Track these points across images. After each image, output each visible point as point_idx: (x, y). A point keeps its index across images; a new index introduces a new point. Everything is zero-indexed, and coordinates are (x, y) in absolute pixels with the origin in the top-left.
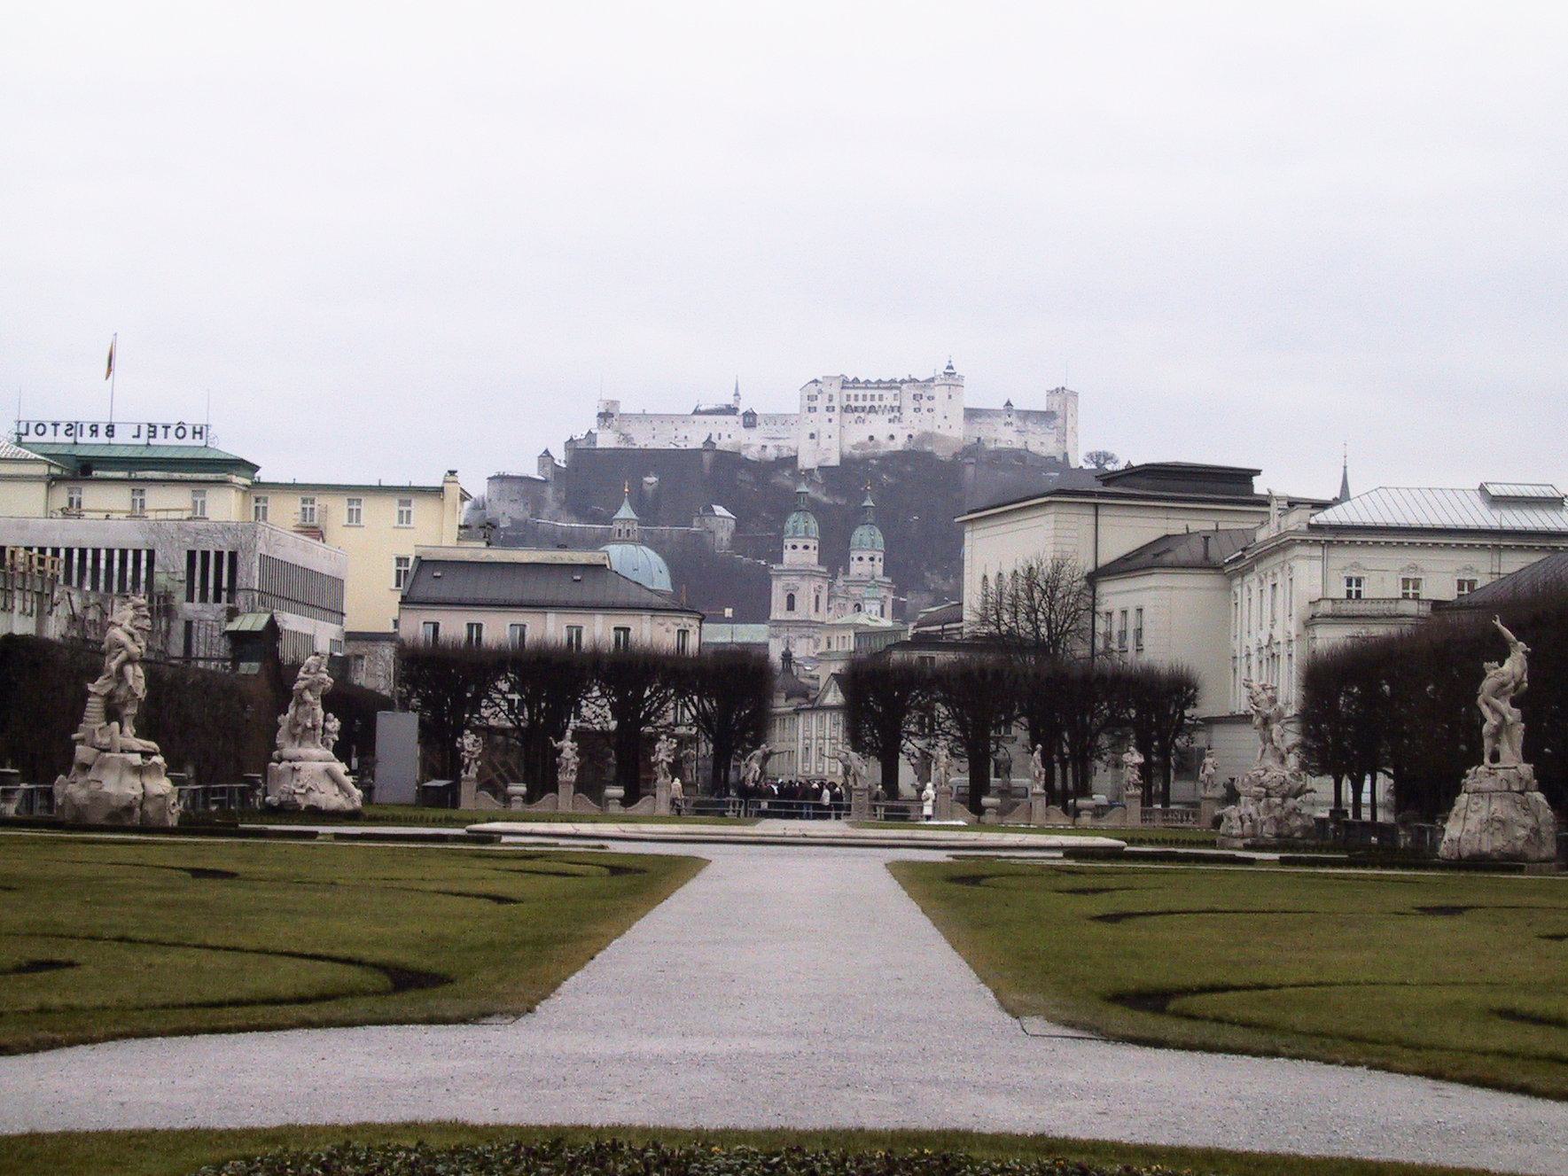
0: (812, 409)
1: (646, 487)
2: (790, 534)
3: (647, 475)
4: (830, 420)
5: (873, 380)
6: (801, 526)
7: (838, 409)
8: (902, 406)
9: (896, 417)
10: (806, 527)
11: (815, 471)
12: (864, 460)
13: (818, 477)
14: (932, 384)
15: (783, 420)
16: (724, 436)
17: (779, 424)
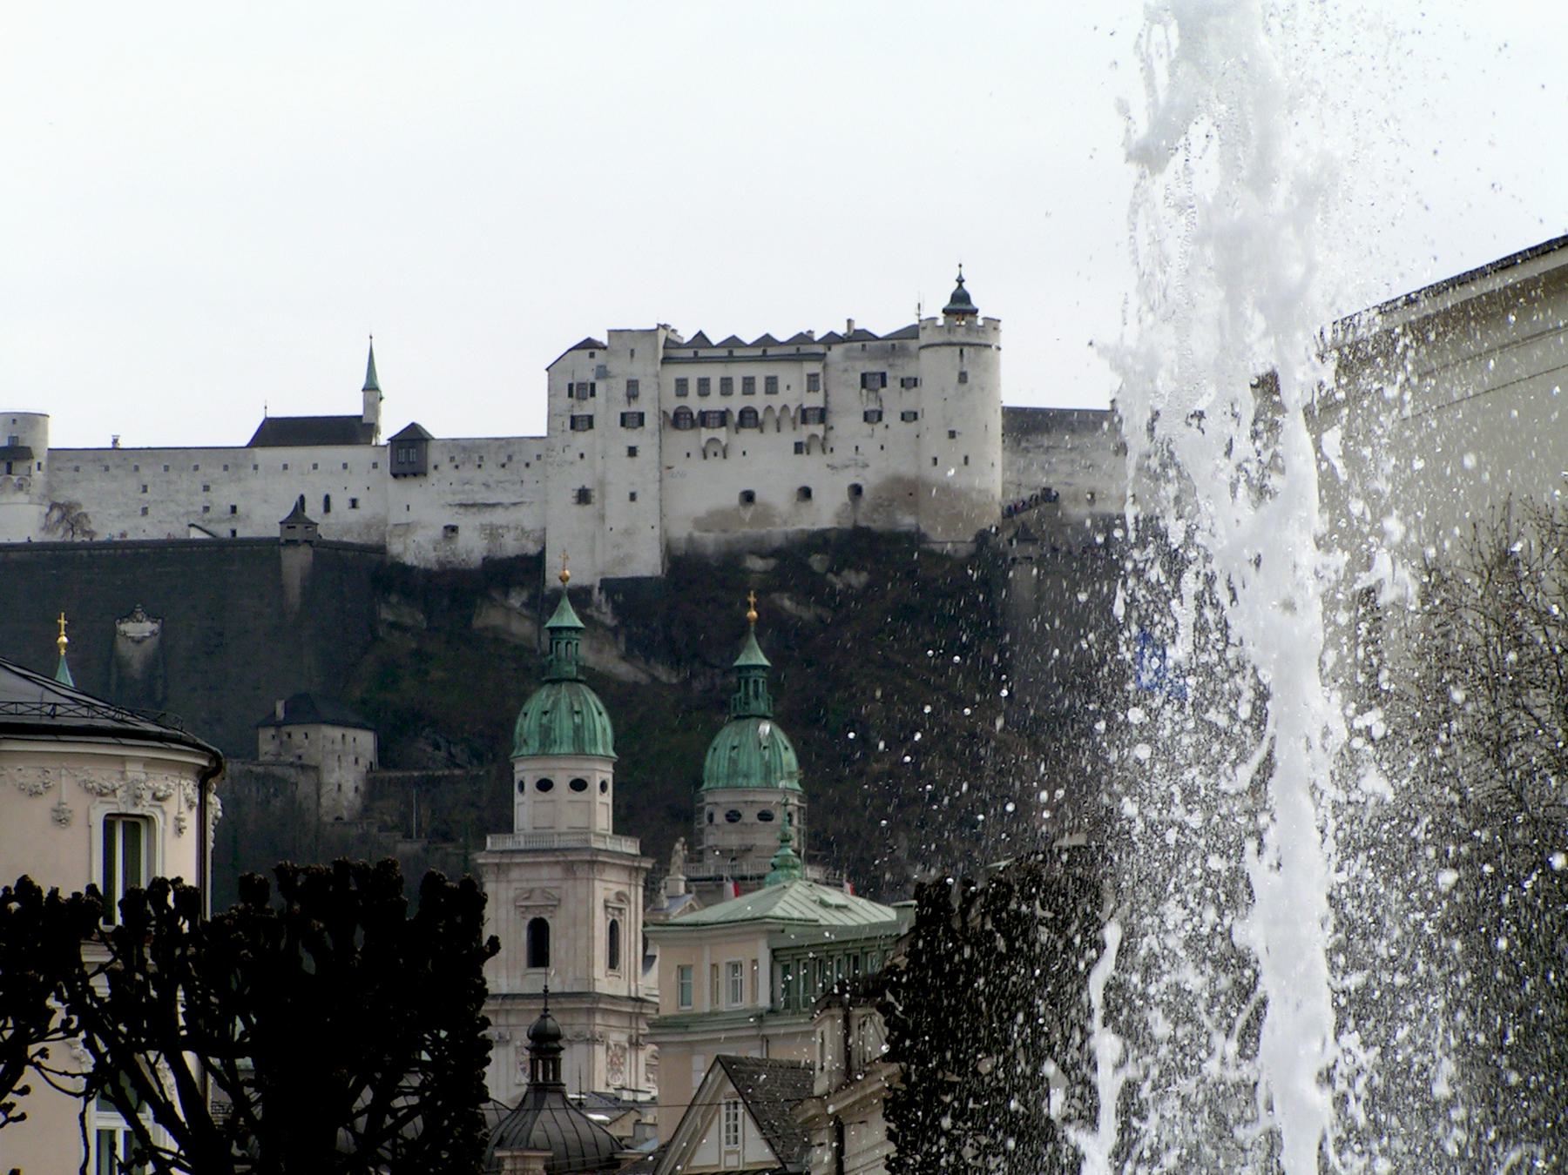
0: (580, 423)
1: (123, 647)
2: (534, 745)
3: (130, 616)
4: (632, 452)
5: (749, 338)
6: (564, 725)
7: (651, 421)
8: (831, 407)
9: (813, 436)
10: (578, 729)
11: (596, 591)
12: (731, 560)
13: (606, 609)
14: (913, 345)
15: (505, 451)
16: (340, 503)
17: (487, 464)
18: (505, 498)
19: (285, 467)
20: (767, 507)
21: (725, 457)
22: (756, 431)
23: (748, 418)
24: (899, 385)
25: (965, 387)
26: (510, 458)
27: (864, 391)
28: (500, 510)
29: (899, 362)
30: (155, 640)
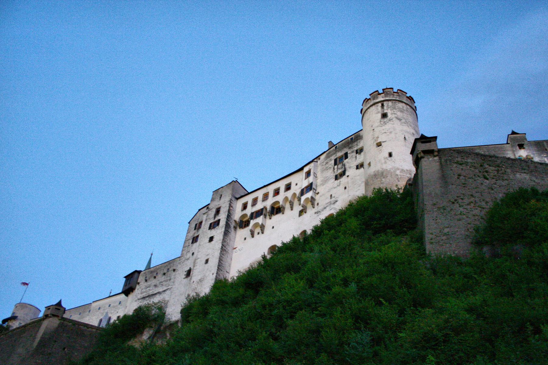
7: (223, 223)
18: (160, 289)
21: (263, 233)
23: (276, 210)
24: (354, 154)
25: (385, 120)
27: (336, 167)
28: (157, 296)
29: (356, 143)
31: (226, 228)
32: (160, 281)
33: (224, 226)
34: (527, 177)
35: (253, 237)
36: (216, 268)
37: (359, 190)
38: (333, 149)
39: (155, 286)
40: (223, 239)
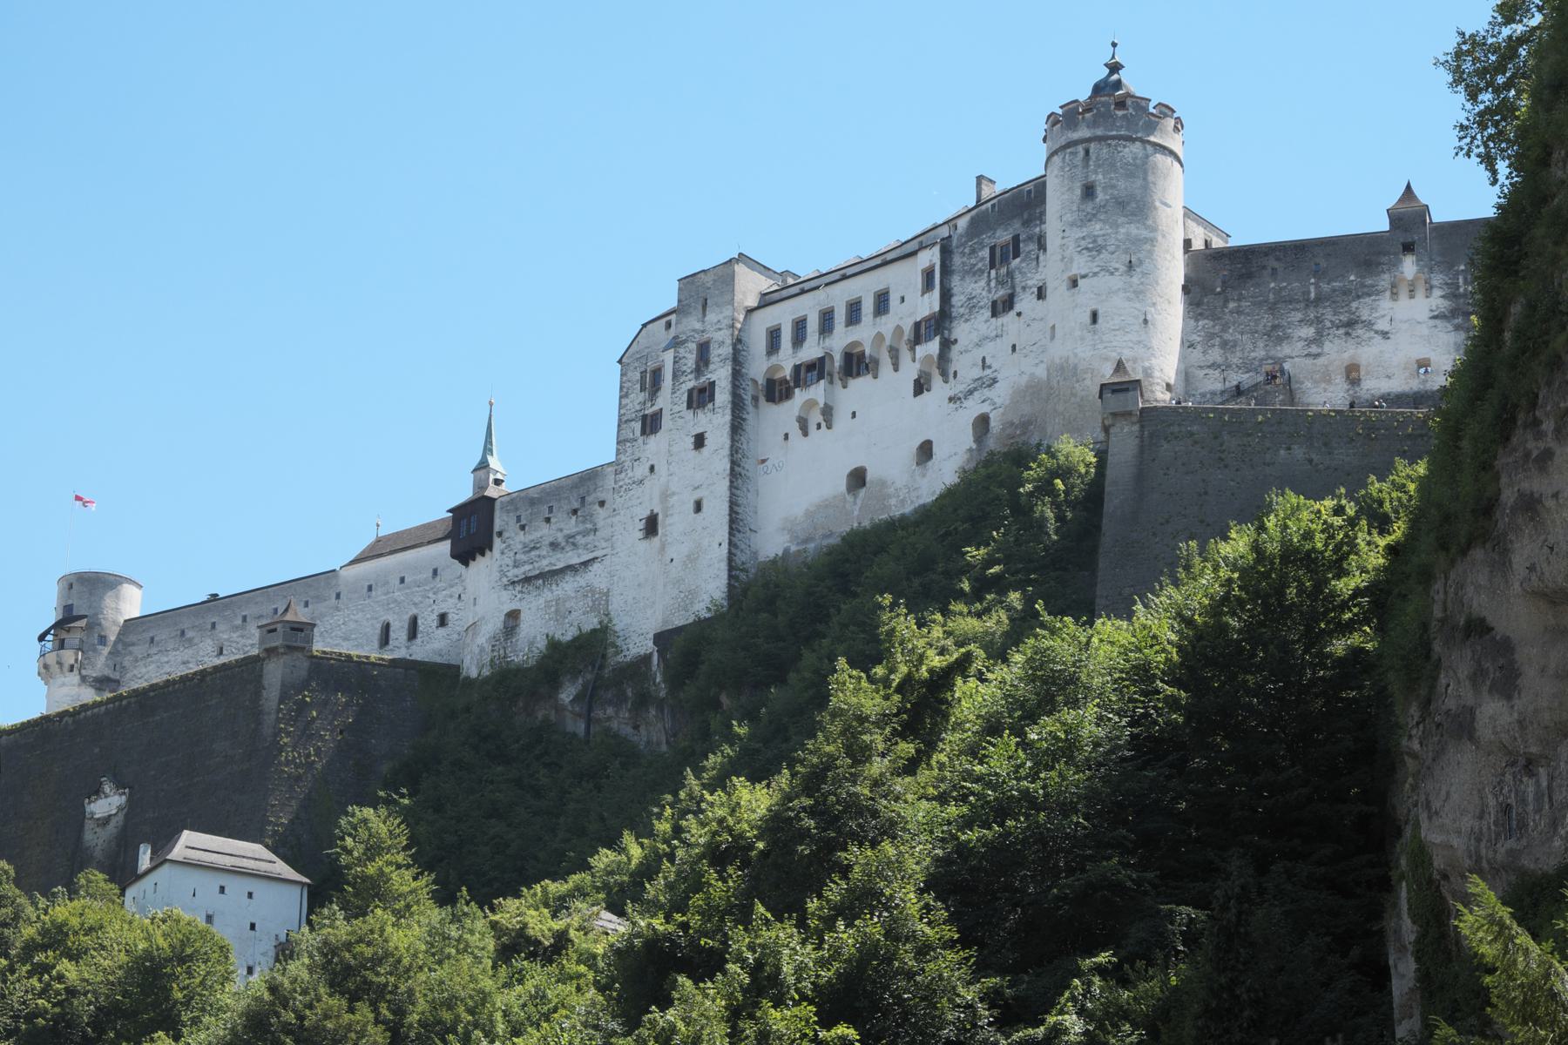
0: (651, 424)
3: (97, 792)
4: (699, 441)
7: (723, 396)
16: (428, 621)
18: (575, 561)
19: (370, 588)
20: (883, 483)
21: (829, 427)
22: (869, 377)
23: (856, 364)
24: (1033, 246)
25: (1089, 207)
26: (583, 499)
27: (993, 272)
30: (121, 817)
31: (733, 411)
32: (566, 532)
33: (730, 406)
34: (1299, 452)
35: (805, 434)
36: (726, 528)
37: (1042, 362)
38: (987, 209)
39: (554, 546)
40: (732, 446)
